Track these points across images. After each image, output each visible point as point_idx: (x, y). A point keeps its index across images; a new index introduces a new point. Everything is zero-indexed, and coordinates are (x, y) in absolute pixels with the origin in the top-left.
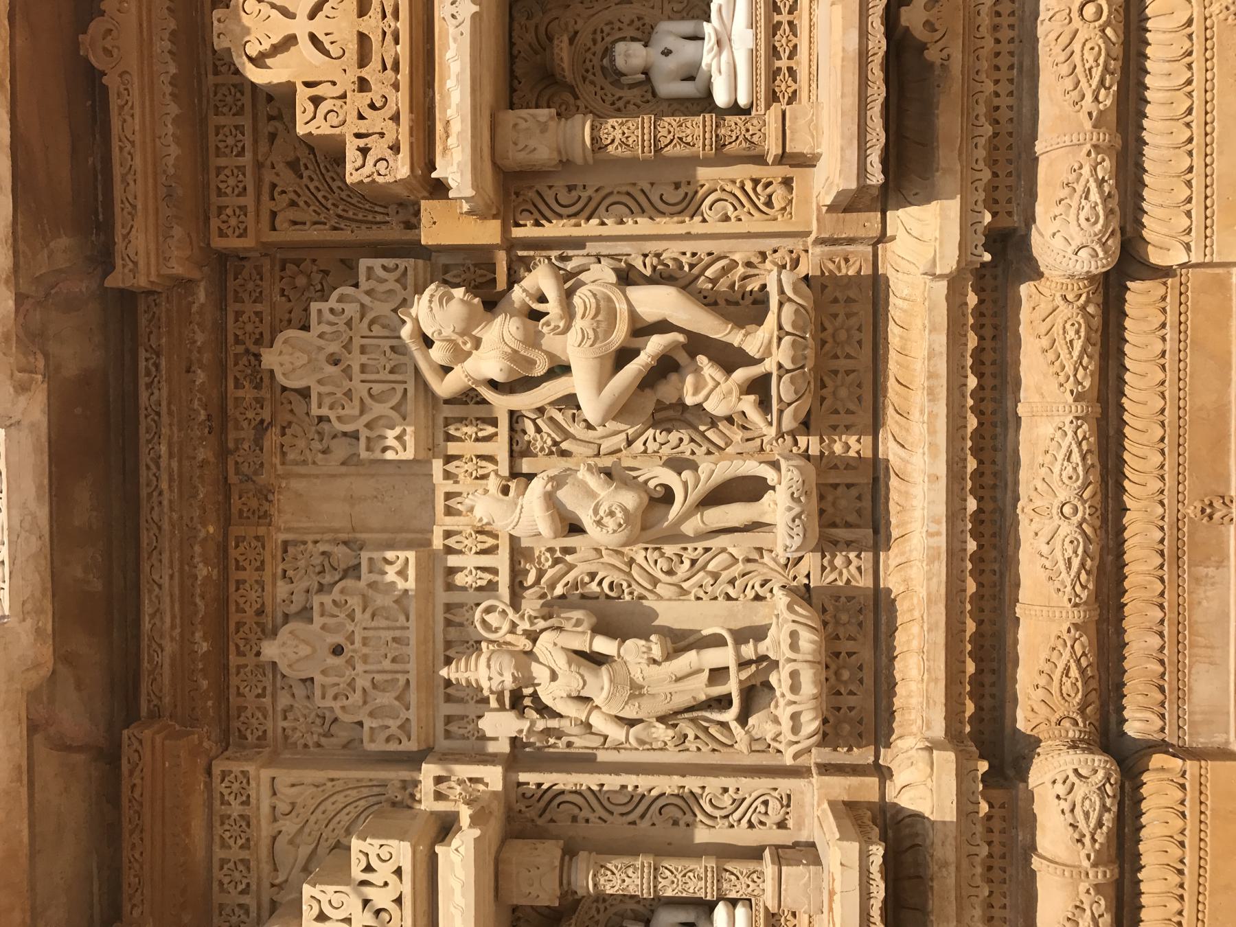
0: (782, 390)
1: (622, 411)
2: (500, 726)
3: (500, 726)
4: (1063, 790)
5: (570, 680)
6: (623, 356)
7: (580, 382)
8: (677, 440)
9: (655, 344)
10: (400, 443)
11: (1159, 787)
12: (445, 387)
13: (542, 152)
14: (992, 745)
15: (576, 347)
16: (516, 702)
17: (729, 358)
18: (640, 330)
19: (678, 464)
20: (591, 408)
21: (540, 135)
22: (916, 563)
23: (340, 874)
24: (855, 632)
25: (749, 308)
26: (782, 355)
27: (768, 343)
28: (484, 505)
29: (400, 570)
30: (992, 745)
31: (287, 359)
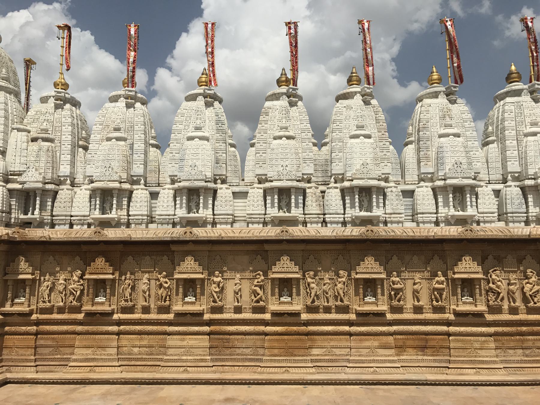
9: (75, 293)
10: (69, 269)
16: (45, 279)
17: (74, 299)
18: (76, 292)
21: (92, 283)
23: (29, 266)
24: (49, 311)
26: (73, 304)
29: (58, 269)
30: (38, 323)
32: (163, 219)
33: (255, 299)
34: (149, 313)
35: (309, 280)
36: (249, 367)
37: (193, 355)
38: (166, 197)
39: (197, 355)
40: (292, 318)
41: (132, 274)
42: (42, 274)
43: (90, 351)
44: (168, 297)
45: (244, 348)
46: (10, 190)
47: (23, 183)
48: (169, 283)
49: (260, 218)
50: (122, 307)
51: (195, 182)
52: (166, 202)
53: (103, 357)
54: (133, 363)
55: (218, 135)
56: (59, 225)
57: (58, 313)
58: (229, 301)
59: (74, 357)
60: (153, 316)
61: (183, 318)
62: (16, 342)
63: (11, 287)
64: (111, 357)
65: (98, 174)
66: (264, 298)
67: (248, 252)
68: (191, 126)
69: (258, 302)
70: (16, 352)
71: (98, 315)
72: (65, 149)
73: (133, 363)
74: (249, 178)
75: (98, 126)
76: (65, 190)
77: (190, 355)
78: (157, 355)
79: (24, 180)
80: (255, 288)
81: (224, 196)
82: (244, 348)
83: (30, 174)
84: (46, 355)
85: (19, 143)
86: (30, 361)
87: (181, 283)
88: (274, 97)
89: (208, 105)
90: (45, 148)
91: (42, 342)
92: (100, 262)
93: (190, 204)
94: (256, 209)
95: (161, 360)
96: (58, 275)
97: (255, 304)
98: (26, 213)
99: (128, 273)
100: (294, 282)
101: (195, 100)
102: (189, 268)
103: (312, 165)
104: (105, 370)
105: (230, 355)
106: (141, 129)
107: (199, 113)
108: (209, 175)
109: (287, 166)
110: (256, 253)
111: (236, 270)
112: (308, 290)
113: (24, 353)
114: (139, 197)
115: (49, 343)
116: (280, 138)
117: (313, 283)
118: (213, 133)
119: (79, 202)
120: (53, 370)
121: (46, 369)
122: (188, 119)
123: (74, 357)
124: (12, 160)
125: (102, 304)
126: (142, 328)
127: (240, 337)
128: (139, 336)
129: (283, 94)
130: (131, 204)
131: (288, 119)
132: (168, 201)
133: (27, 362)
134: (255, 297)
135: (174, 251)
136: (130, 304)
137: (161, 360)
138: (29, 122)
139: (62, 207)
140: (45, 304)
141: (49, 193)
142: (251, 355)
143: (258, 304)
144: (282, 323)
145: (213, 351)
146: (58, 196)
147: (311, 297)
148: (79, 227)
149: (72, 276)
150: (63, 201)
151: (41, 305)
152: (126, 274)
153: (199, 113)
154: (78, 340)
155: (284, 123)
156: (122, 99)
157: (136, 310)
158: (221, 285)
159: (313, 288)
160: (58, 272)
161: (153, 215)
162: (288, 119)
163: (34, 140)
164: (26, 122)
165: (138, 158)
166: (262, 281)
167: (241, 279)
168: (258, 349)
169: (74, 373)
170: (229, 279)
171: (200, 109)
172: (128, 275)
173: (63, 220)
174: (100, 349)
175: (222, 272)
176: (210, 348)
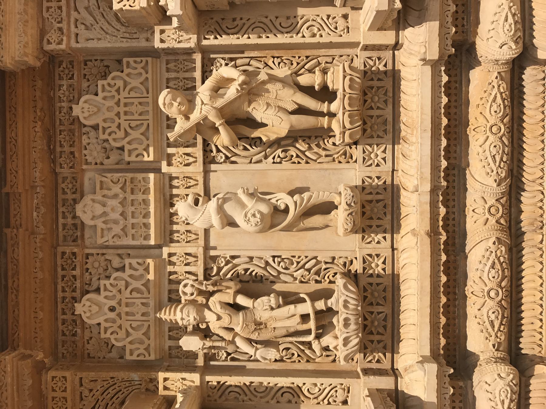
44: (304, 80)
50: (364, 348)
99: (165, 315)
136: (343, 298)
152: (177, 331)
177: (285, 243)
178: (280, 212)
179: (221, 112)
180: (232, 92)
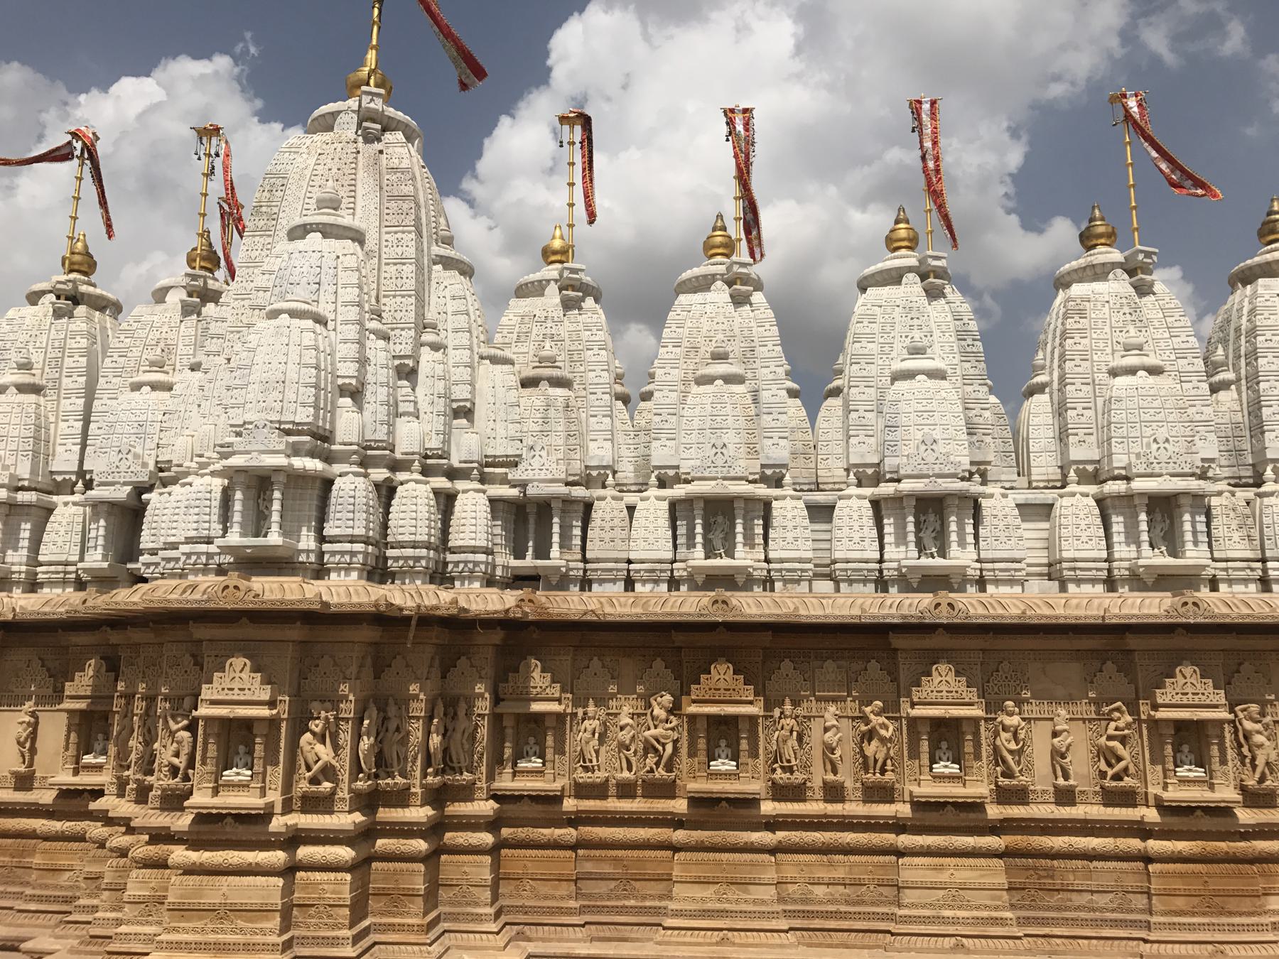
0: (650, 775)
1: (646, 740)
2: (580, 711)
3: (580, 711)
4: (569, 834)
5: (590, 728)
6: (658, 741)
7: (653, 731)
8: (641, 752)
9: (660, 748)
11: (569, 853)
12: (652, 700)
13: (698, 726)
14: (576, 820)
15: (659, 731)
16: (585, 713)
17: (657, 764)
18: (664, 745)
19: (635, 752)
20: (647, 733)
21: (701, 725)
22: (614, 804)
23: (553, 681)
24: (599, 791)
25: (669, 768)
26: (657, 776)
27: (661, 773)
28: (627, 709)
29: (613, 689)
30: (576, 820)
31: (659, 664)
32: (854, 570)
33: (1110, 772)
34: (842, 800)
35: (1248, 725)
36: (1116, 942)
37: (971, 908)
38: (855, 517)
39: (978, 908)
40: (1216, 820)
41: (796, 704)
42: (580, 702)
43: (709, 892)
44: (889, 762)
45: (1092, 892)
46: (492, 501)
47: (523, 485)
48: (891, 729)
49: (1098, 570)
51: (940, 481)
52: (856, 528)
53: (744, 907)
54: (817, 923)
55: (967, 365)
56: (601, 581)
57: (620, 796)
58: (1040, 776)
59: (672, 905)
60: (854, 808)
61: (933, 815)
62: (529, 864)
63: (509, 731)
64: (763, 908)
65: (698, 463)
66: (1132, 769)
67: (1078, 655)
68: (898, 346)
69: (1117, 777)
70: (533, 889)
71: (724, 804)
72: (597, 403)
73: (817, 923)
74: (1043, 470)
75: (670, 349)
76: (609, 499)
77: (960, 908)
78: (873, 904)
79: (524, 477)
80: (1111, 744)
81: (1000, 514)
82: (1092, 892)
83: (536, 463)
84: (601, 897)
85: (501, 391)
86: (569, 912)
87: (924, 729)
88: (1089, 272)
89: (934, 294)
90: (560, 403)
91: (589, 867)
92: (722, 674)
93: (921, 535)
94: (1087, 546)
95: (890, 917)
96: (613, 703)
97: (1114, 784)
98: (519, 554)
99: (787, 700)
100: (1211, 731)
101: (898, 281)
102: (944, 692)
103: (1212, 437)
104: (757, 941)
105: (1059, 909)
106: (774, 354)
107: (914, 314)
108: (965, 462)
109: (1167, 440)
110: (1101, 656)
111: (1053, 699)
112: (1245, 750)
113: (551, 892)
114: (789, 517)
115: (607, 869)
116: (1132, 371)
117: (1259, 732)
118: (955, 361)
119: (646, 528)
120: (627, 935)
121: (608, 934)
122: (888, 329)
123: (672, 905)
124: (489, 430)
125: (727, 775)
126: (821, 837)
127: (1079, 863)
128: (825, 858)
129: (1114, 265)
130: (772, 534)
131: (1142, 325)
132: (861, 527)
133: (552, 914)
134: (1110, 765)
135: (896, 650)
136: (798, 777)
137: (890, 917)
138: (507, 340)
139: (607, 540)
140: (589, 774)
141: (576, 507)
142: (1113, 911)
143: (1122, 784)
144: (1219, 832)
145: (1017, 895)
146: (594, 515)
147: (1254, 767)
148: (649, 587)
149: (649, 706)
150: (607, 526)
151: (583, 777)
153: (914, 314)
154: (680, 865)
155: (1133, 335)
156: (719, 283)
157: (809, 793)
158: (1022, 735)
159: (1260, 746)
160: (613, 696)
161: (825, 562)
162: (1142, 325)
163: (528, 383)
164: (501, 340)
165: (773, 424)
166: (1128, 726)
167: (1071, 719)
168: (1130, 896)
169: (684, 944)
170: (1035, 719)
171: (913, 304)
172: (788, 707)
173: (611, 570)
174: (733, 887)
175: (1019, 703)
176: (1009, 889)
177: (817, 754)
178: (832, 751)
179: (874, 728)
180: (883, 732)
